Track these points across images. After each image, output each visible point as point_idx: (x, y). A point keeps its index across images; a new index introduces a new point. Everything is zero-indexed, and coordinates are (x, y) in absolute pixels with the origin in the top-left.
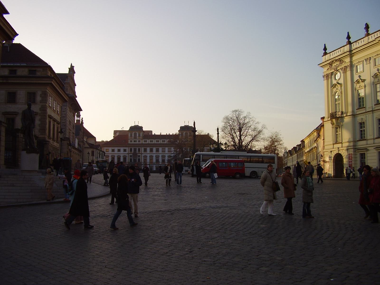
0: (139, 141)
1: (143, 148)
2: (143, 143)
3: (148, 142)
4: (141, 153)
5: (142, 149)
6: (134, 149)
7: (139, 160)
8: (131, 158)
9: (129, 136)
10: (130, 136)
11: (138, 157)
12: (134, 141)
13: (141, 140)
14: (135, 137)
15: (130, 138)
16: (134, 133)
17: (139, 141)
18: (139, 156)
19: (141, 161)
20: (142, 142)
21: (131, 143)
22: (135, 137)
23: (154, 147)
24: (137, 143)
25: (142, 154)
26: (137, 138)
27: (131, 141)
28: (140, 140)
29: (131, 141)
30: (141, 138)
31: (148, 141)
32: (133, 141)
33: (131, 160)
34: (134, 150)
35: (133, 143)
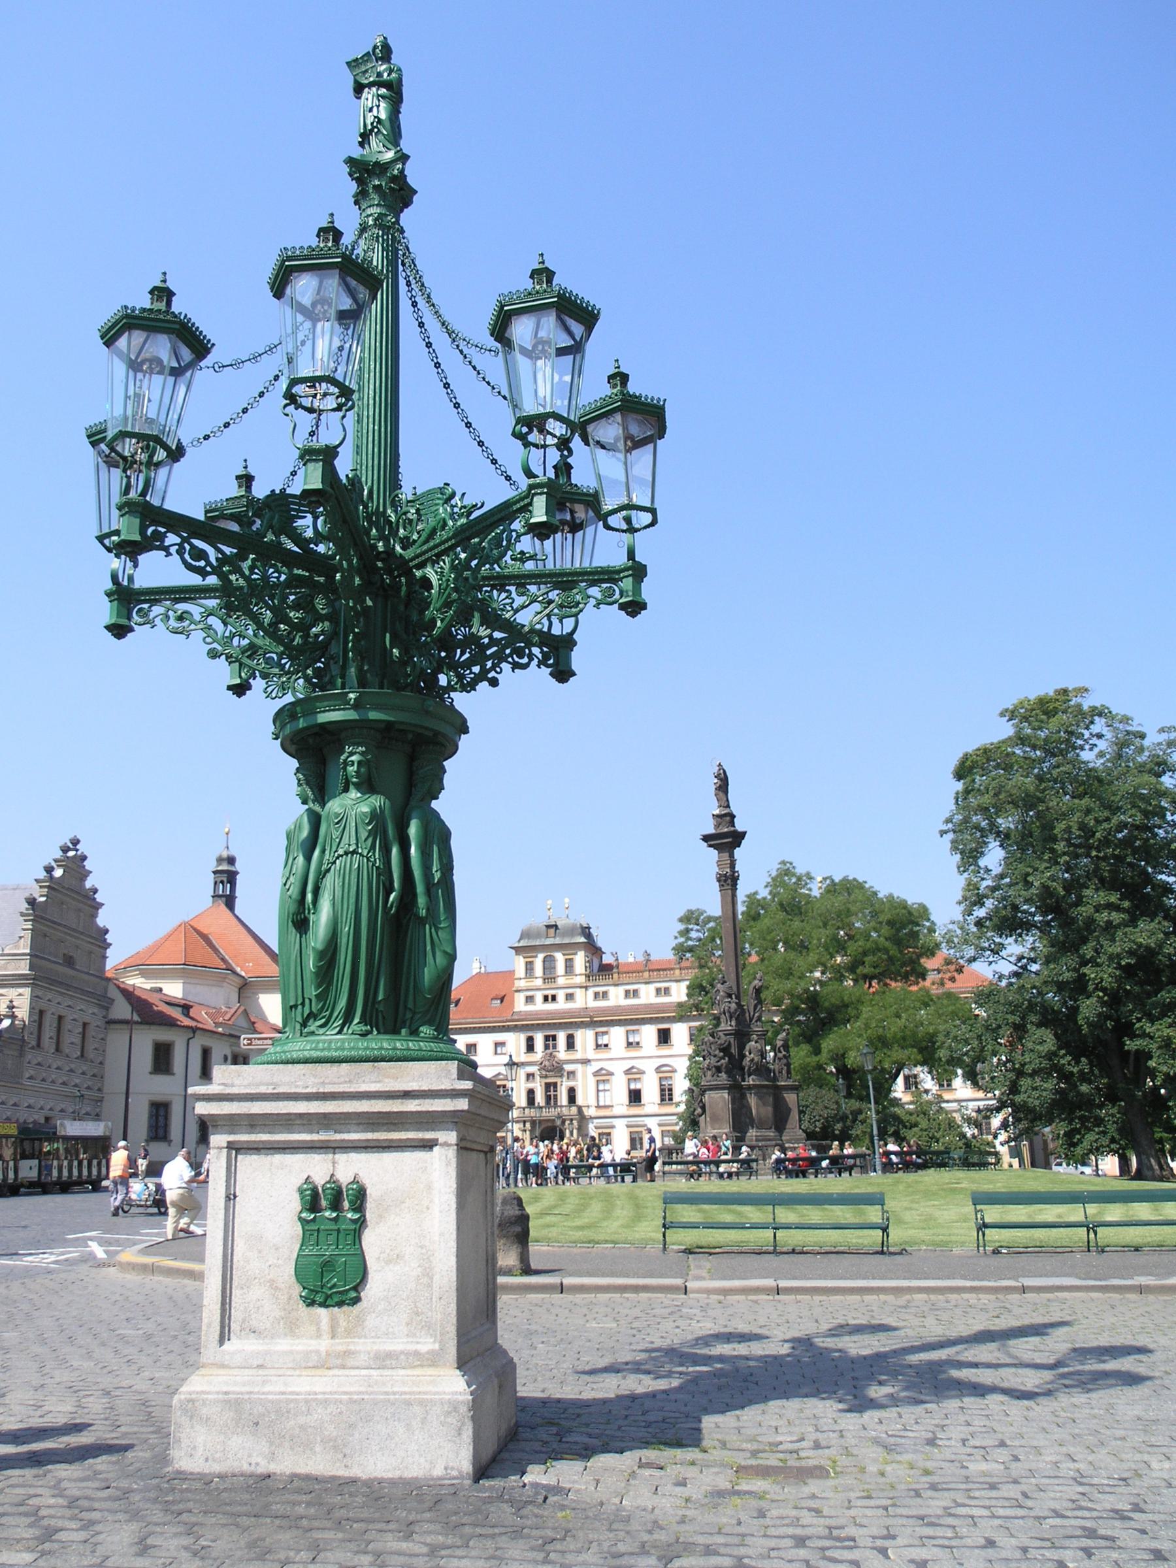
0: (570, 997)
1: (589, 1034)
2: (593, 1004)
3: (617, 997)
4: (579, 1055)
5: (585, 1038)
6: (547, 1038)
7: (572, 1092)
8: (531, 1085)
9: (520, 971)
10: (523, 975)
11: (565, 1079)
12: (546, 998)
13: (578, 990)
14: (549, 976)
15: (522, 984)
16: (541, 956)
17: (570, 997)
18: (571, 1074)
19: (580, 1101)
20: (585, 1000)
21: (530, 1008)
22: (549, 976)
23: (643, 1021)
24: (561, 1005)
25: (586, 1062)
26: (561, 981)
27: (530, 999)
28: (570, 991)
29: (530, 999)
30: (580, 980)
31: (616, 997)
32: (539, 997)
33: (531, 1093)
34: (547, 1047)
35: (539, 1006)
